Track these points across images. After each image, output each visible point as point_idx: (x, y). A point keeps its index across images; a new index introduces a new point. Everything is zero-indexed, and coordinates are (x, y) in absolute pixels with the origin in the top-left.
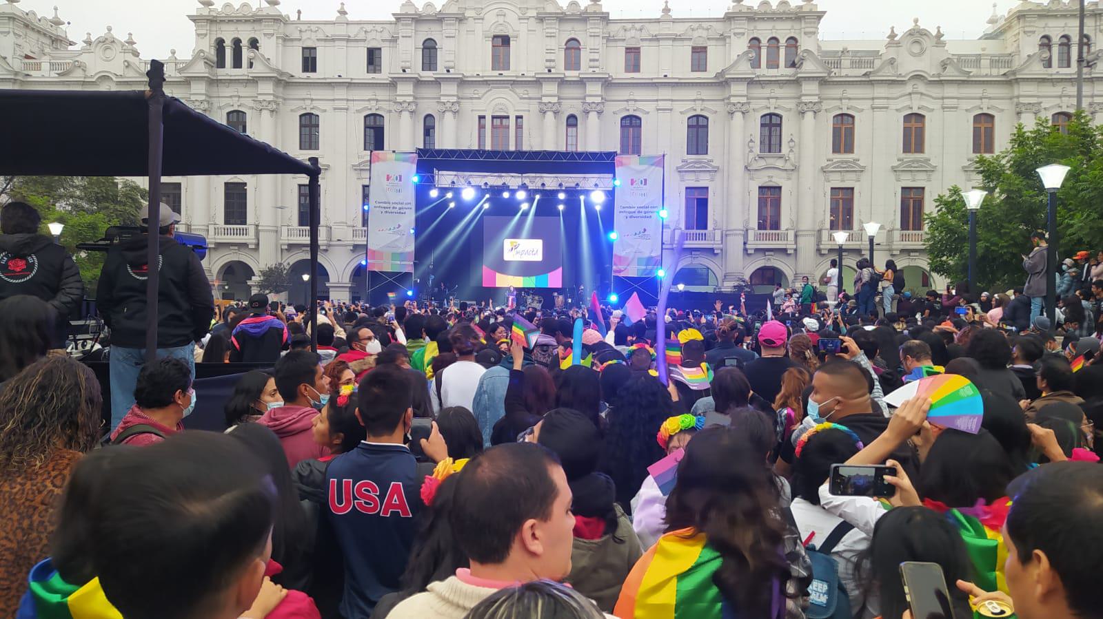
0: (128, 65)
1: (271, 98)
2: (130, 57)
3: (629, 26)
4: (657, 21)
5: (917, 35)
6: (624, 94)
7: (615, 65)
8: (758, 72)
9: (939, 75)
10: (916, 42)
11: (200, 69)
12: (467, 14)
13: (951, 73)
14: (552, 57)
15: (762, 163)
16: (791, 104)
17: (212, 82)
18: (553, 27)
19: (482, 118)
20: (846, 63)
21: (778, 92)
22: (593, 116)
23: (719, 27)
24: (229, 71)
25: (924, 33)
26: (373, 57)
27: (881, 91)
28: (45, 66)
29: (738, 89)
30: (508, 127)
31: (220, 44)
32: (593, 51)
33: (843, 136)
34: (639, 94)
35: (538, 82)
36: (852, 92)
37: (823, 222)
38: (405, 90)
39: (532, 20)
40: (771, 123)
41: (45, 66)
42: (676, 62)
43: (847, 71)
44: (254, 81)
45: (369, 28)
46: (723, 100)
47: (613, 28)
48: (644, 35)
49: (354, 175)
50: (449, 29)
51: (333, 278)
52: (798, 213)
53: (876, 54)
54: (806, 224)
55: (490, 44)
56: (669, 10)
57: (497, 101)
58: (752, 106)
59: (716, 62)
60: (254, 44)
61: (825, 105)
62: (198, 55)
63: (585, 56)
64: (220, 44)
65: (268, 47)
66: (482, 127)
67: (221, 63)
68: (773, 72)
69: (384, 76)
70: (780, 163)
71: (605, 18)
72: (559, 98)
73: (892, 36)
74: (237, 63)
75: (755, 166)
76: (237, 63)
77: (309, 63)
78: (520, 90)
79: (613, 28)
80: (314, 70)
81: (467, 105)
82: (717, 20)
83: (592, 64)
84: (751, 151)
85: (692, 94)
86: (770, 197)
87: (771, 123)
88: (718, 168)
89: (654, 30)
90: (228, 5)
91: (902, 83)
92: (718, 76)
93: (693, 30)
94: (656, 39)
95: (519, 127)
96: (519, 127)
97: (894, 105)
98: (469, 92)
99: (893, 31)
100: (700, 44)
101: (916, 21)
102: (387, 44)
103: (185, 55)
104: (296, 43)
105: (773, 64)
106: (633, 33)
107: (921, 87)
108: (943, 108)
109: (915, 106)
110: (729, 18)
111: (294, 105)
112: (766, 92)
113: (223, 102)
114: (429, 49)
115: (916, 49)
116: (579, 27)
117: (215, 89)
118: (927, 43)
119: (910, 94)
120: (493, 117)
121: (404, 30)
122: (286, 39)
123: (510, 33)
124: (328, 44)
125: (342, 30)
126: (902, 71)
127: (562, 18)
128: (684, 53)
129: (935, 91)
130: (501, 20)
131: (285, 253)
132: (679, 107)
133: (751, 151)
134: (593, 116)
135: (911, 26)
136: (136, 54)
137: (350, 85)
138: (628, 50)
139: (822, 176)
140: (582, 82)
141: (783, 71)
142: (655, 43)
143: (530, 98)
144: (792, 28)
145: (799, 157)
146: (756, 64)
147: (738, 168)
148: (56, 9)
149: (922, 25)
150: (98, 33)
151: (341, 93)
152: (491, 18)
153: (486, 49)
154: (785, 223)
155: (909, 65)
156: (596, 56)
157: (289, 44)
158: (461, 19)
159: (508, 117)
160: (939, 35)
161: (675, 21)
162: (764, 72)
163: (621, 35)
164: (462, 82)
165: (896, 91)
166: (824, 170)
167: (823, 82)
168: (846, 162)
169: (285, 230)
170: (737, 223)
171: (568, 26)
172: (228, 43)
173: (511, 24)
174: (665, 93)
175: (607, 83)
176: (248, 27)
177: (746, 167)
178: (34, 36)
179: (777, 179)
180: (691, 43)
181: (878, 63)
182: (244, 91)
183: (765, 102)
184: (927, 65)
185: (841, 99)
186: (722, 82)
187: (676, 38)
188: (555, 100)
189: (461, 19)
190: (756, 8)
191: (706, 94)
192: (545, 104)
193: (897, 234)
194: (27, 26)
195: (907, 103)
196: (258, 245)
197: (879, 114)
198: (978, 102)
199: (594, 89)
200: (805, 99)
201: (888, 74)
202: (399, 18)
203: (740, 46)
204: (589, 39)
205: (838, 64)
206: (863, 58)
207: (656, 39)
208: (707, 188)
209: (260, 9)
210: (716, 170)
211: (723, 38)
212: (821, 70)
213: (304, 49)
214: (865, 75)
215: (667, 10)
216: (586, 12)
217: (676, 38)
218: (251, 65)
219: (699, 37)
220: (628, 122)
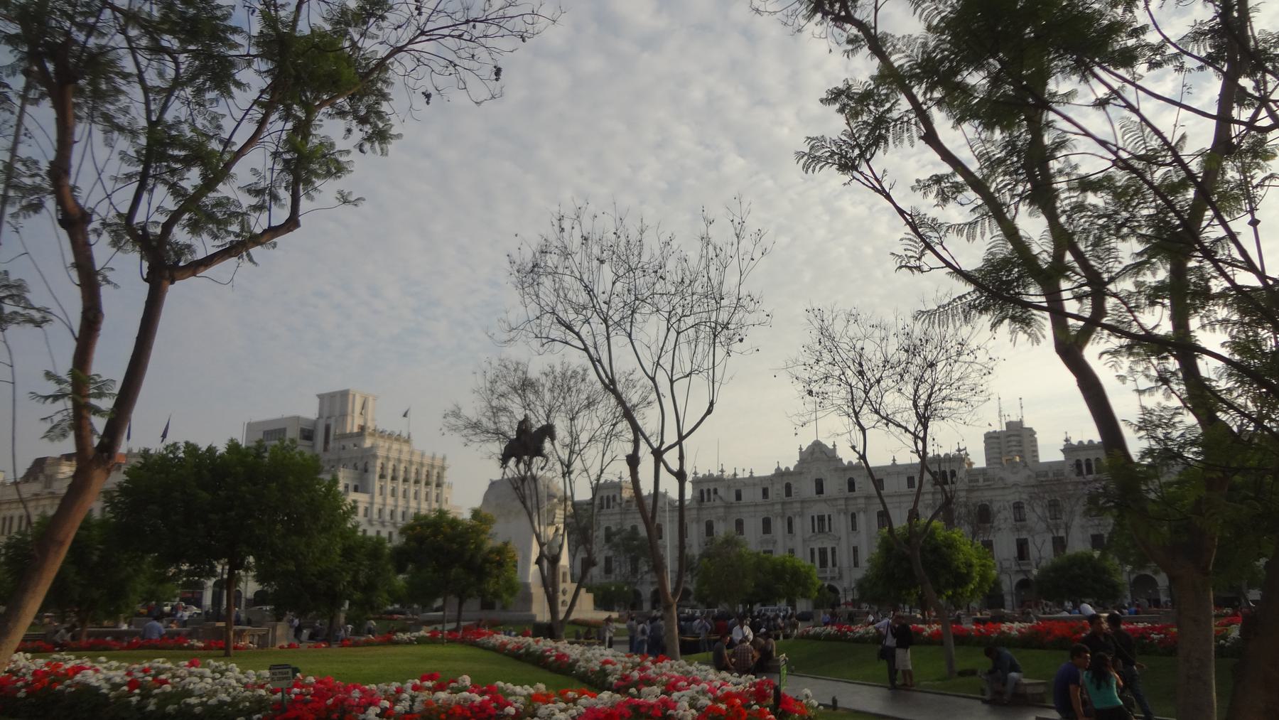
11: (695, 505)
26: (765, 492)
35: (836, 499)
60: (716, 491)
64: (702, 492)
65: (721, 492)
67: (702, 500)
77: (739, 497)
114: (788, 488)
125: (752, 481)
137: (756, 505)
140: (855, 498)
151: (752, 509)
158: (801, 473)
164: (802, 502)
189: (801, 473)
202: (773, 476)
217: (899, 473)
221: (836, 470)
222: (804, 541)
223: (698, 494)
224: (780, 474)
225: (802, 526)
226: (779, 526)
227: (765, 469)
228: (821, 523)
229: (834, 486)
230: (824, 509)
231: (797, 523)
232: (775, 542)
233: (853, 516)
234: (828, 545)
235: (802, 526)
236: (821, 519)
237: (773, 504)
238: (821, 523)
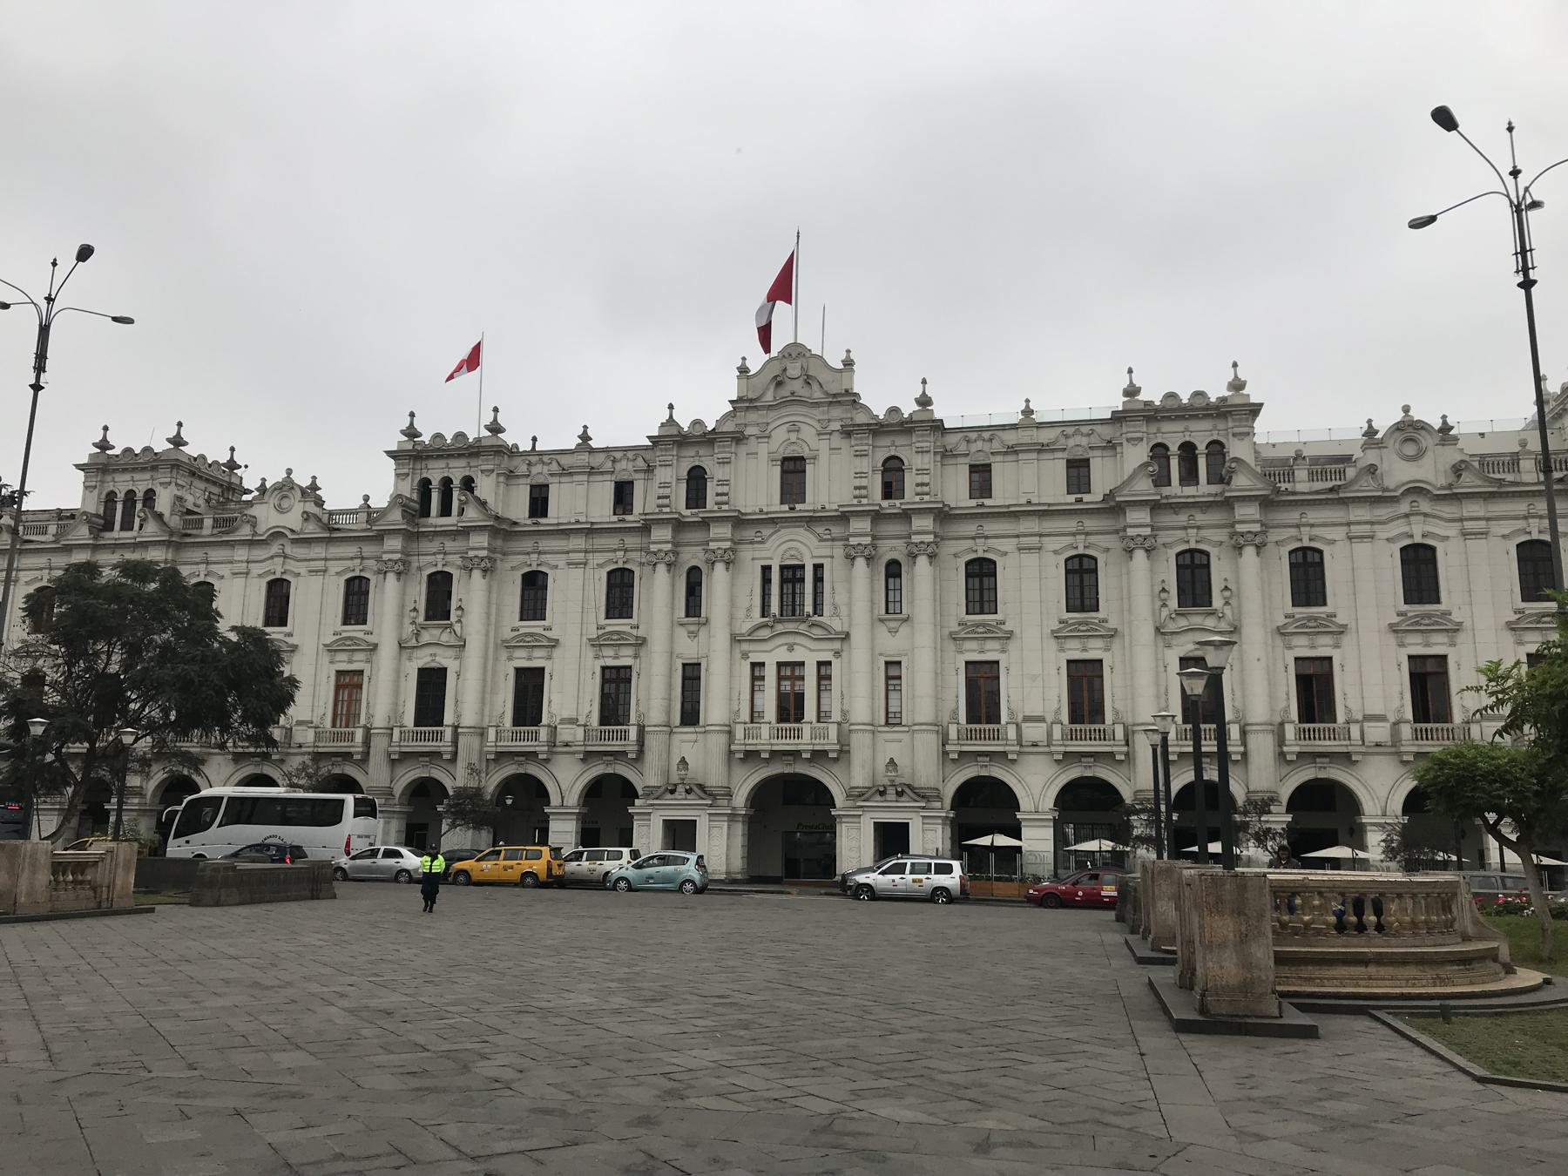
0: (307, 516)
1: (484, 553)
2: (311, 508)
3: (973, 436)
4: (1014, 427)
5: (1409, 429)
6: (970, 528)
7: (955, 489)
8: (1166, 491)
9: (1450, 486)
10: (1407, 440)
12: (749, 431)
13: (1469, 482)
14: (864, 482)
15: (1183, 623)
17: (412, 536)
18: (865, 444)
19: (766, 570)
20: (1301, 474)
21: (1200, 518)
22: (922, 561)
23: (1107, 432)
24: (435, 520)
25: (1421, 426)
26: (623, 495)
27: (1359, 513)
28: (208, 522)
29: (1139, 516)
30: (802, 580)
31: (425, 485)
33: (1308, 577)
34: (991, 527)
35: (844, 517)
36: (1313, 515)
37: (1287, 710)
38: (662, 534)
39: (836, 436)
41: (208, 522)
42: (1044, 481)
43: (1302, 483)
44: (465, 532)
45: (618, 455)
46: (1117, 532)
47: (951, 440)
48: (996, 446)
49: (590, 653)
50: (720, 451)
51: (555, 800)
52: (1244, 696)
53: (1346, 459)
54: (1259, 711)
55: (777, 470)
56: (1032, 412)
57: (785, 547)
58: (1160, 541)
59: (1103, 477)
60: (468, 484)
61: (1274, 536)
62: (397, 499)
63: (910, 480)
64: (425, 485)
65: (486, 487)
66: (766, 581)
67: (425, 512)
68: (1190, 490)
69: (633, 519)
70: (1210, 622)
71: (938, 427)
72: (874, 538)
73: (1371, 432)
74: (446, 511)
75: (1171, 627)
76: (446, 511)
77: (539, 505)
78: (820, 530)
79: (951, 440)
80: (545, 515)
81: (746, 553)
82: (1102, 422)
83: (919, 489)
84: (1164, 605)
85: (1070, 524)
88: (1116, 630)
89: (1011, 438)
90: (438, 436)
91: (1393, 500)
92: (1106, 497)
93: (1067, 437)
94: (1012, 451)
95: (818, 579)
96: (818, 579)
97: (1383, 532)
98: (749, 533)
99: (1370, 426)
100: (1079, 454)
101: (1406, 409)
102: (642, 475)
103: (380, 501)
104: (522, 481)
105: (1189, 476)
106: (979, 445)
107: (1425, 506)
108: (1464, 535)
109: (1418, 531)
110: (1118, 418)
111: (517, 560)
112: (1182, 518)
113: (424, 560)
114: (697, 481)
115: (1410, 449)
116: (900, 440)
117: (415, 545)
118: (1427, 441)
119: (1407, 516)
120: (782, 568)
121: (659, 456)
122: (510, 476)
123: (806, 453)
124: (563, 479)
126: (1390, 482)
127: (878, 429)
128: (1056, 470)
129: (1448, 510)
130: (793, 437)
131: (492, 766)
132: (1051, 544)
133: (1164, 605)
134: (922, 561)
135: (1399, 416)
136: (319, 502)
137: (591, 531)
138: (973, 469)
139: (1279, 641)
140: (906, 516)
141: (1204, 489)
142: (1013, 458)
143: (833, 540)
144: (1215, 428)
145: (1240, 613)
146: (1162, 480)
147: (1145, 632)
148: (232, 449)
149: (1416, 415)
150: (275, 477)
151: (578, 542)
152: (780, 434)
155: (1399, 472)
156: (926, 479)
157: (514, 481)
158: (739, 438)
159: (802, 567)
160: (1446, 428)
161: (1041, 426)
162: (1176, 489)
163: (963, 448)
164: (739, 521)
165: (1383, 512)
166: (1281, 632)
167: (1266, 503)
168: (1316, 619)
169: (492, 733)
170: (1145, 711)
171: (885, 441)
172: (435, 483)
173: (809, 440)
175: (944, 515)
176: (462, 463)
177: (1157, 630)
178: (201, 485)
180: (1065, 455)
181: (1351, 473)
182: (450, 545)
183: (1180, 534)
184: (1432, 469)
185: (1298, 526)
186: (1113, 507)
187: (1042, 449)
188: (867, 540)
190: (1157, 403)
191: (1090, 523)
192: (854, 547)
193: (1406, 731)
194: (193, 474)
195: (1405, 529)
196: (455, 754)
197: (1362, 548)
198: (1521, 524)
199: (924, 523)
200: (1240, 528)
201: (1367, 487)
203: (1137, 455)
204: (917, 459)
205: (1290, 476)
206: (1332, 464)
207: (1012, 451)
208: (1101, 661)
209: (478, 440)
210: (1113, 634)
211: (1111, 446)
212: (1260, 486)
213: (532, 487)
214: (1331, 490)
216: (910, 420)
217: (1042, 449)
218: (461, 512)
219: (1078, 444)
220: (976, 568)
222: (735, 639)
223: (408, 489)
224: (672, 439)
225: (732, 595)
226: (658, 595)
227: (627, 425)
228: (792, 590)
229: (837, 479)
230: (805, 547)
231: (717, 584)
232: (641, 642)
234: (808, 654)
235: (732, 595)
236: (792, 574)
237: (645, 528)
238: (792, 590)
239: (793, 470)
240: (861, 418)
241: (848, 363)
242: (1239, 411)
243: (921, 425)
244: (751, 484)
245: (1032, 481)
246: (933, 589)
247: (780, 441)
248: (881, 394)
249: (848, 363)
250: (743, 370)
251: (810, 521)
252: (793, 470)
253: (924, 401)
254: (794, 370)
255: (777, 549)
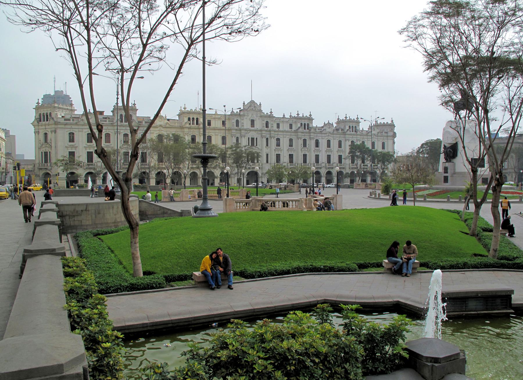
16: (308, 137)
27: (323, 135)
32: (272, 124)
34: (280, 133)
35: (261, 131)
40: (305, 141)
59: (294, 128)
63: (269, 125)
76: (193, 124)
85: (289, 134)
86: (305, 156)
87: (305, 141)
114: (237, 122)
116: (269, 118)
129: (332, 135)
132: (287, 136)
140: (270, 131)
152: (250, 115)
153: (250, 123)
154: (308, 162)
155: (328, 130)
158: (244, 115)
165: (326, 135)
173: (254, 117)
174: (285, 133)
179: (306, 153)
191: (292, 134)
203: (299, 125)
205: (316, 129)
215: (284, 115)
219: (291, 122)
221: (261, 117)
230: (254, 135)
233: (267, 139)
236: (253, 139)
239: (253, 122)
240: (262, 114)
241: (260, 104)
242: (310, 119)
243: (271, 116)
244: (246, 124)
245: (284, 127)
246: (273, 142)
247: (250, 117)
248: (266, 110)
249: (260, 104)
250: (244, 103)
251: (255, 131)
252: (253, 122)
253: (271, 112)
254: (253, 105)
255: (251, 135)
